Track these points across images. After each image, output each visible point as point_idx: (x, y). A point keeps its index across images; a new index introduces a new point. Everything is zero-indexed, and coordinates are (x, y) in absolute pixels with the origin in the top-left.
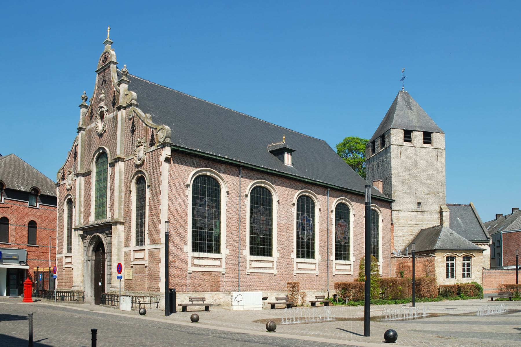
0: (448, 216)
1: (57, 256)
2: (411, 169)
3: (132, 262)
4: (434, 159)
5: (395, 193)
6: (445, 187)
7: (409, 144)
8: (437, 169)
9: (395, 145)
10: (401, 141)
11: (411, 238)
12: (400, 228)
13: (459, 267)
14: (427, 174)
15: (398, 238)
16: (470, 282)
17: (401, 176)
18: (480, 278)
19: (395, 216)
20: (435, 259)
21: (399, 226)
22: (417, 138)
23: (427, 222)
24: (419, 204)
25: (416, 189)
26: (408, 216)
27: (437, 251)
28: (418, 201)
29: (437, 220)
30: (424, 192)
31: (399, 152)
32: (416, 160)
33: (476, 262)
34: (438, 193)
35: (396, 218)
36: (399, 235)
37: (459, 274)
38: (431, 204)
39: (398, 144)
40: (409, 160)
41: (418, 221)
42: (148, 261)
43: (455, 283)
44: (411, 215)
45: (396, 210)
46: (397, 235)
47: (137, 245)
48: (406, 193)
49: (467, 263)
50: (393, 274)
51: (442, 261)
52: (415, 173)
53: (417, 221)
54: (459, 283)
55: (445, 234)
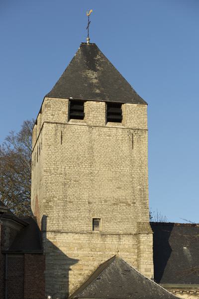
4: (125, 147)
7: (79, 122)
8: (132, 162)
11: (80, 279)
14: (113, 170)
22: (94, 113)
24: (95, 222)
26: (74, 241)
28: (93, 215)
29: (132, 250)
30: (106, 201)
31: (59, 134)
34: (134, 203)
36: (56, 273)
44: (79, 239)
52: (89, 169)
53: (91, 250)
55: (112, 271)
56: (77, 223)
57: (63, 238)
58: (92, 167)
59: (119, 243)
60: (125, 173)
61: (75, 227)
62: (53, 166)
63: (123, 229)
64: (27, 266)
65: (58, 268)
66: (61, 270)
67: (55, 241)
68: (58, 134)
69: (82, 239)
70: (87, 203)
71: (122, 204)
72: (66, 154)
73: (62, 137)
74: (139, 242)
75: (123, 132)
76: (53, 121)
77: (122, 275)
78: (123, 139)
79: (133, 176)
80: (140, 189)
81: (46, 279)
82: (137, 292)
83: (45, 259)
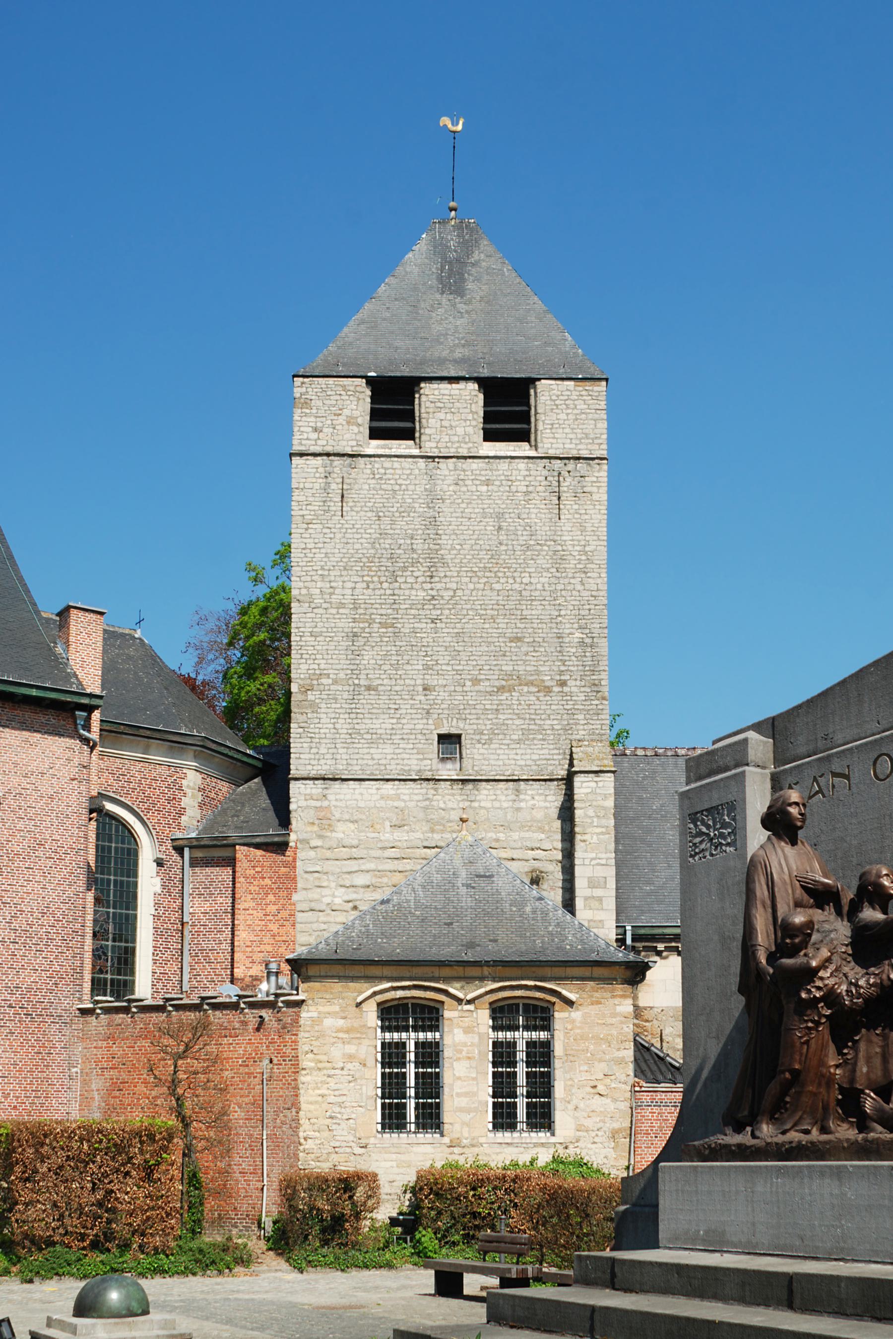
0: (605, 797)
2: (404, 569)
5: (305, 690)
6: (603, 646)
8: (559, 559)
9: (315, 455)
10: (347, 436)
12: (329, 866)
13: (466, 1063)
14: (497, 586)
15: (322, 917)
16: (544, 1158)
17: (342, 605)
18: (614, 1135)
19: (307, 807)
20: (304, 1015)
21: (328, 854)
22: (441, 415)
23: (490, 835)
25: (427, 667)
26: (382, 803)
27: (312, 971)
30: (476, 681)
31: (335, 487)
33: (584, 1038)
34: (563, 684)
35: (310, 815)
37: (468, 1111)
39: (329, 449)
40: (393, 523)
41: (442, 831)
43: (438, 1165)
44: (398, 797)
45: (313, 774)
46: (314, 905)
48: (369, 688)
49: (530, 1044)
50: (86, 1100)
51: (347, 1031)
52: (429, 586)
53: (432, 831)
54: (465, 1159)
56: (389, 749)
57: (348, 797)
58: (437, 579)
59: (517, 805)
60: (537, 593)
61: (383, 762)
62: (319, 585)
63: (529, 763)
64: (242, 880)
65: (333, 885)
66: (343, 890)
67: (325, 804)
68: (333, 486)
69: (406, 798)
70: (420, 689)
71: (526, 689)
72: (357, 546)
73: (343, 496)
75: (529, 470)
77: (463, 891)
78: (531, 489)
79: (561, 601)
80: (582, 643)
81: (300, 917)
82: (495, 941)
83: (294, 860)
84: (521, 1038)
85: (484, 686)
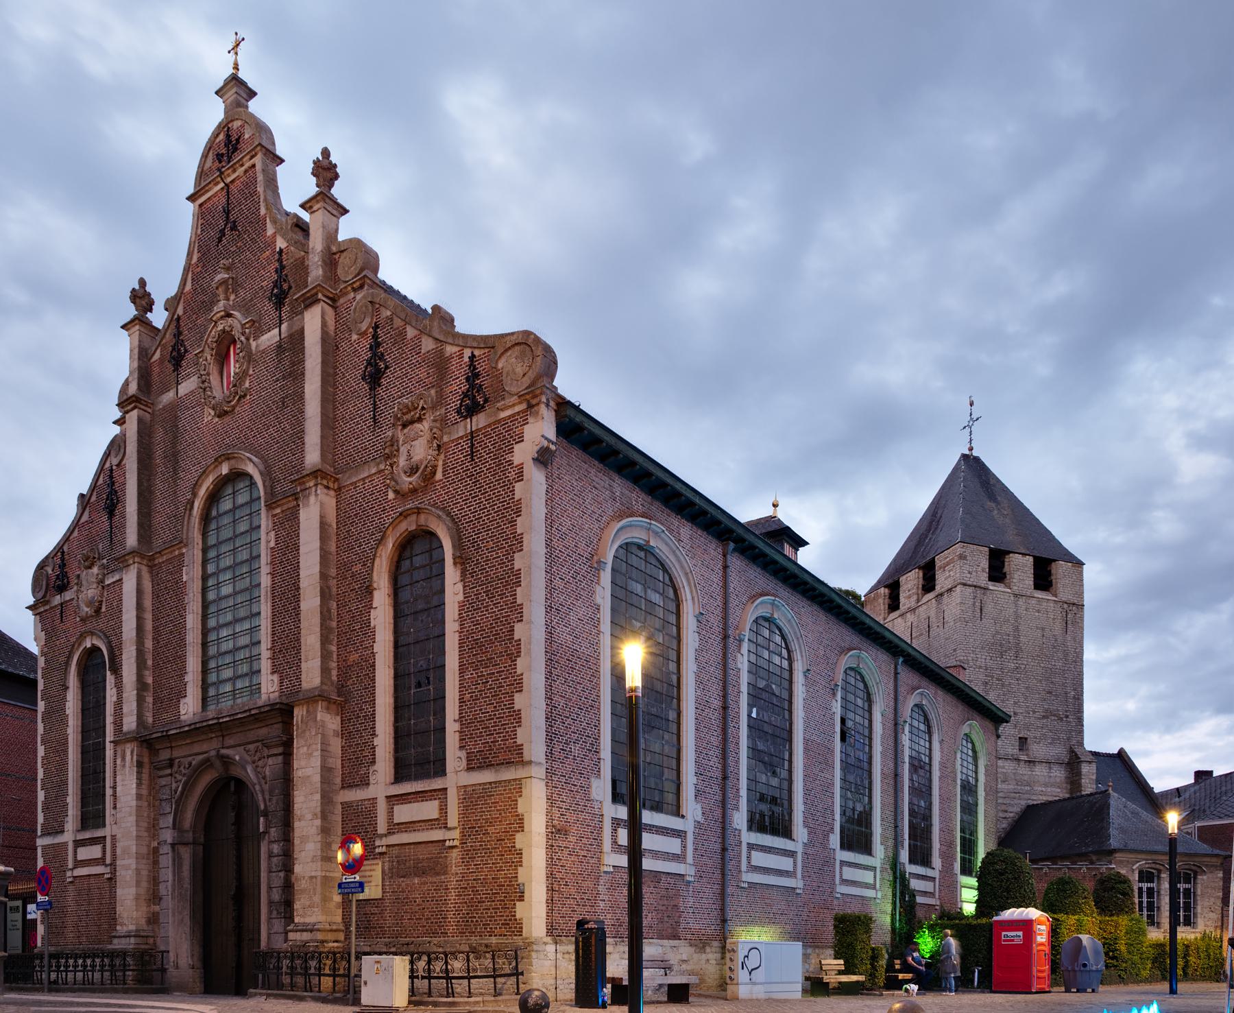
1: (40, 842)
2: (1006, 651)
3: (382, 836)
9: (970, 586)
14: (1042, 665)
17: (980, 667)
25: (1015, 703)
30: (1034, 712)
32: (1017, 629)
34: (1067, 717)
38: (1050, 744)
42: (458, 831)
47: (399, 778)
52: (1015, 661)
71: (1053, 718)
74: (1079, 774)
76: (971, 583)
84: (1181, 886)
85: (1037, 715)
